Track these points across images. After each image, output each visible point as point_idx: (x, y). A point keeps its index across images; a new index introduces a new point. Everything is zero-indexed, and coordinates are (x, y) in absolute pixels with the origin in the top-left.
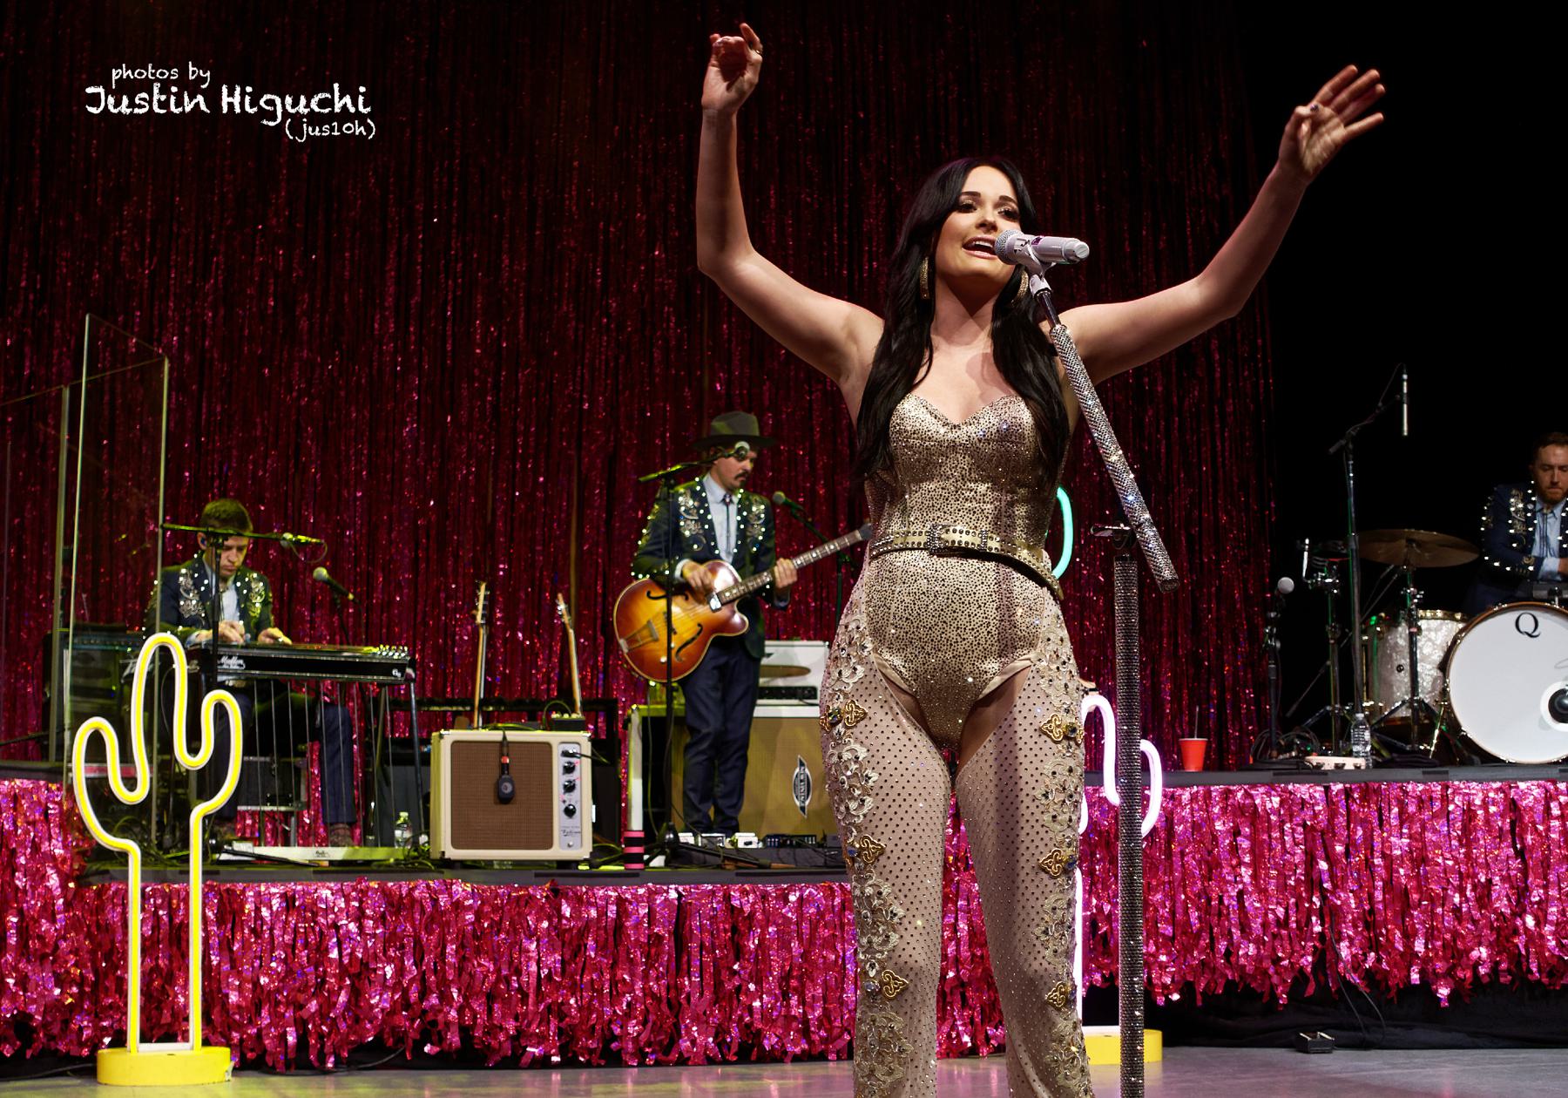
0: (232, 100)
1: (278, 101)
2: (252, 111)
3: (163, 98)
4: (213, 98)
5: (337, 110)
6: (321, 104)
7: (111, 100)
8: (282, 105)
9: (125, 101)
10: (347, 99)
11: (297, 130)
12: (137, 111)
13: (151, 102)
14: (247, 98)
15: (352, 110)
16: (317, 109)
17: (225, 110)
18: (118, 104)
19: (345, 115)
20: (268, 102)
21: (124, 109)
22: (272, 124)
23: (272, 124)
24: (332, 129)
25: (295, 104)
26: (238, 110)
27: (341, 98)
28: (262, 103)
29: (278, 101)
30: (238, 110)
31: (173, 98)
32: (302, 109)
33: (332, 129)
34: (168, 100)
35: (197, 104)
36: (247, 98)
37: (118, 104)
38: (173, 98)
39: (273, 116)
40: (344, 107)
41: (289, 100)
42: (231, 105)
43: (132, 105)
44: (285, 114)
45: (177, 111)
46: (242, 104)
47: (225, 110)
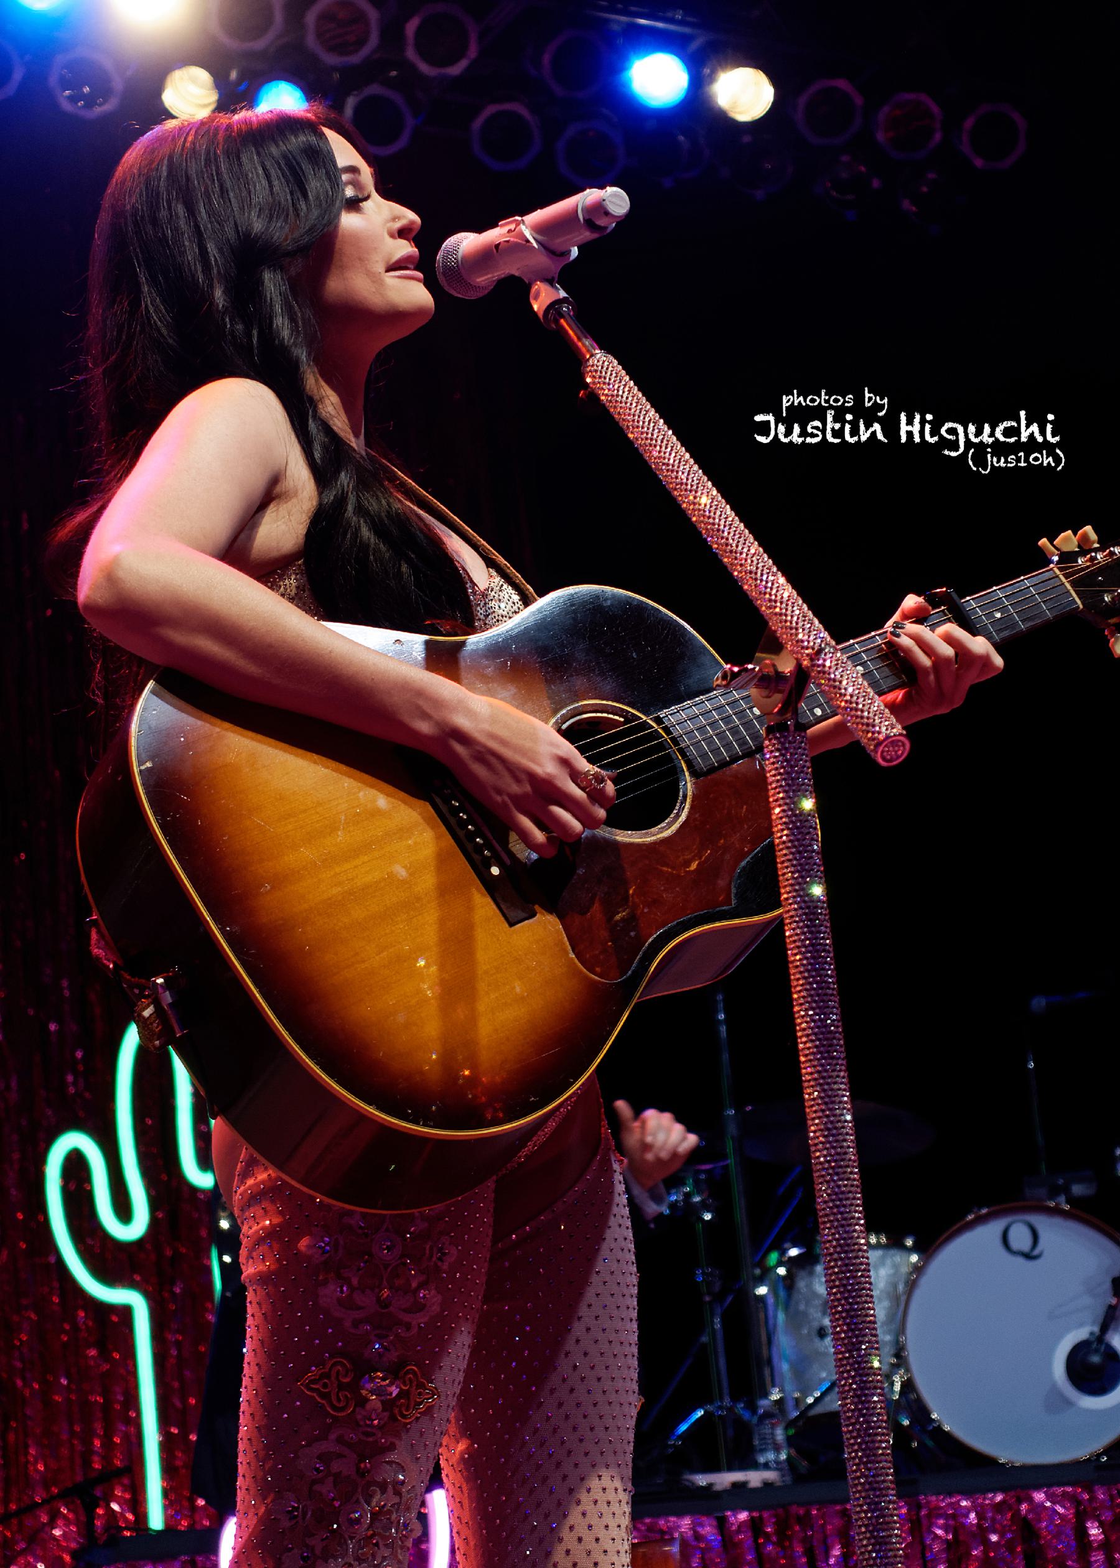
0: (911, 428)
1: (960, 429)
3: (837, 426)
4: (891, 427)
6: (1007, 432)
7: (782, 428)
8: (965, 433)
9: (797, 429)
11: (980, 460)
12: (809, 440)
13: (824, 431)
14: (928, 427)
16: (1002, 439)
17: (904, 439)
18: (789, 433)
20: (949, 431)
21: (796, 438)
22: (954, 454)
23: (954, 454)
24: (1018, 460)
25: (979, 433)
26: (917, 439)
28: (943, 431)
29: (960, 429)
30: (917, 439)
31: (848, 427)
32: (986, 438)
33: (1018, 460)
34: (842, 429)
35: (874, 433)
36: (928, 427)
37: (789, 433)
38: (848, 427)
39: (954, 446)
41: (972, 428)
42: (910, 434)
43: (804, 433)
44: (968, 443)
47: (904, 439)
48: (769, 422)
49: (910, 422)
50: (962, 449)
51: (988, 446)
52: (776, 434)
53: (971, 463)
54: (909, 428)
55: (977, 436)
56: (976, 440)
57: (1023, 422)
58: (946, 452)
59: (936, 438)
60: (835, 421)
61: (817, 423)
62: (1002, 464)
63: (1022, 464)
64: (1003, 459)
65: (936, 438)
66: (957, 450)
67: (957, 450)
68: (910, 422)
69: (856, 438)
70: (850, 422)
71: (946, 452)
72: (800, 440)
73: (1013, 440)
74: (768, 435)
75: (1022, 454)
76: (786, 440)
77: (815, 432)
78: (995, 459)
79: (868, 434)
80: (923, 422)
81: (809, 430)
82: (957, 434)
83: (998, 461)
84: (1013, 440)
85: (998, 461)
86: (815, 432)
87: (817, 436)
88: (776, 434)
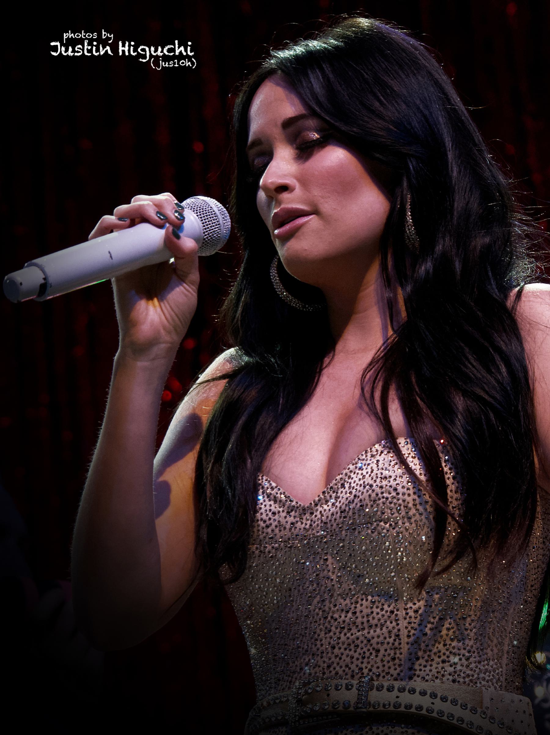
0: (124, 49)
1: (147, 49)
2: (134, 54)
3: (89, 48)
4: (115, 48)
5: (177, 54)
6: (169, 51)
8: (149, 51)
9: (70, 49)
10: (182, 48)
11: (157, 64)
12: (76, 54)
13: (83, 50)
14: (132, 48)
15: (185, 54)
16: (167, 54)
17: (121, 54)
18: (67, 51)
19: (181, 57)
20: (142, 50)
21: (70, 53)
22: (144, 61)
23: (144, 61)
24: (174, 63)
25: (156, 51)
26: (127, 54)
27: (179, 48)
28: (139, 50)
29: (147, 49)
30: (127, 54)
31: (94, 48)
32: (159, 53)
33: (174, 63)
34: (92, 49)
35: (107, 51)
36: (132, 48)
37: (67, 51)
38: (94, 48)
39: (144, 57)
40: (181, 52)
41: (153, 49)
42: (123, 51)
43: (74, 51)
44: (151, 55)
45: (96, 54)
46: (129, 51)
47: (121, 54)
51: (160, 57)
52: (61, 51)
53: (152, 65)
54: (123, 48)
55: (155, 52)
56: (155, 54)
58: (141, 60)
59: (136, 53)
61: (80, 46)
62: (167, 65)
63: (176, 65)
64: (167, 63)
65: (136, 53)
66: (146, 59)
67: (146, 59)
69: (98, 53)
71: (141, 60)
72: (72, 54)
73: (172, 54)
74: (57, 52)
75: (176, 61)
77: (79, 50)
78: (163, 63)
79: (104, 52)
81: (76, 49)
82: (146, 52)
83: (165, 64)
84: (172, 54)
85: (165, 64)
86: (79, 50)
88: (61, 51)
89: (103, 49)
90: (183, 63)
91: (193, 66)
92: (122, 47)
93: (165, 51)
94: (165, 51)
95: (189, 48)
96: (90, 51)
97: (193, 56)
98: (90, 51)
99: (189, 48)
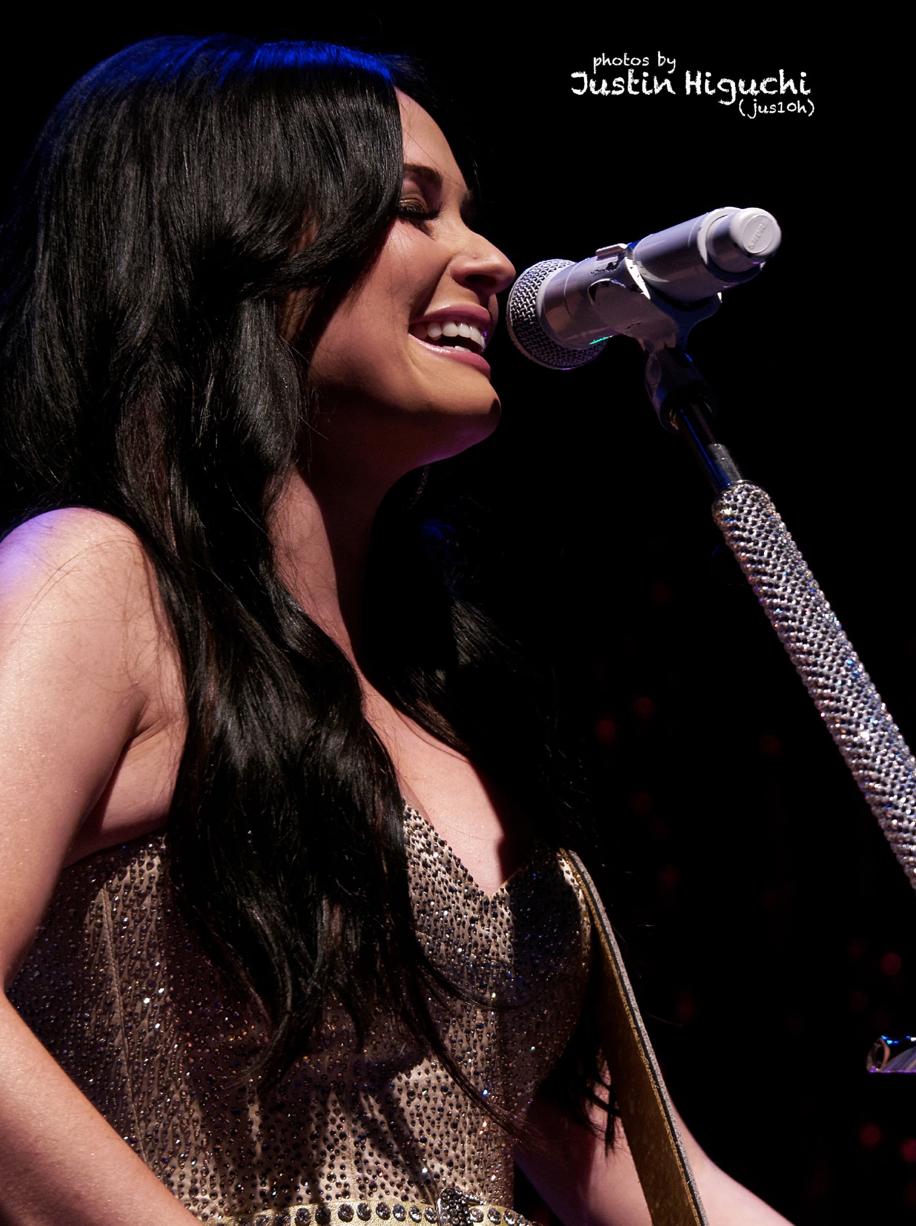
0: (694, 83)
1: (733, 84)
3: (636, 81)
4: (678, 83)
5: (782, 92)
6: (770, 86)
7: (593, 83)
8: (736, 87)
9: (604, 84)
10: (791, 83)
11: (748, 108)
12: (614, 92)
13: (626, 85)
14: (707, 82)
15: (795, 92)
16: (765, 91)
17: (688, 92)
18: (598, 87)
19: (789, 96)
20: (724, 85)
21: (604, 91)
22: (727, 103)
23: (727, 103)
24: (778, 108)
25: (747, 87)
26: (699, 92)
27: (785, 82)
28: (719, 85)
29: (733, 84)
30: (699, 92)
31: (644, 82)
32: (753, 91)
33: (778, 108)
35: (665, 87)
36: (707, 82)
37: (598, 87)
38: (644, 82)
39: (728, 97)
40: (789, 89)
41: (742, 83)
42: (693, 88)
43: (610, 87)
44: (739, 94)
46: (703, 87)
47: (688, 92)
48: (582, 78)
49: (693, 78)
50: (734, 100)
51: (754, 97)
53: (741, 110)
54: (693, 83)
55: (745, 89)
56: (745, 93)
57: (782, 78)
58: (722, 102)
59: (714, 91)
60: (635, 77)
61: (621, 79)
62: (765, 111)
63: (781, 111)
64: (766, 108)
65: (714, 91)
68: (693, 78)
69: (651, 91)
70: (646, 79)
71: (722, 102)
72: (607, 92)
73: (774, 92)
74: (582, 89)
75: (781, 103)
76: (596, 93)
77: (619, 86)
78: (760, 107)
79: (660, 88)
80: (703, 78)
81: (615, 85)
82: (730, 88)
83: (763, 109)
84: (774, 92)
85: (763, 109)
86: (619, 86)
87: (620, 89)
89: (660, 84)
90: (792, 107)
91: (809, 112)
92: (691, 80)
93: (763, 88)
94: (763, 88)
95: (802, 82)
96: (637, 87)
97: (809, 96)
98: (637, 87)
99: (802, 82)
